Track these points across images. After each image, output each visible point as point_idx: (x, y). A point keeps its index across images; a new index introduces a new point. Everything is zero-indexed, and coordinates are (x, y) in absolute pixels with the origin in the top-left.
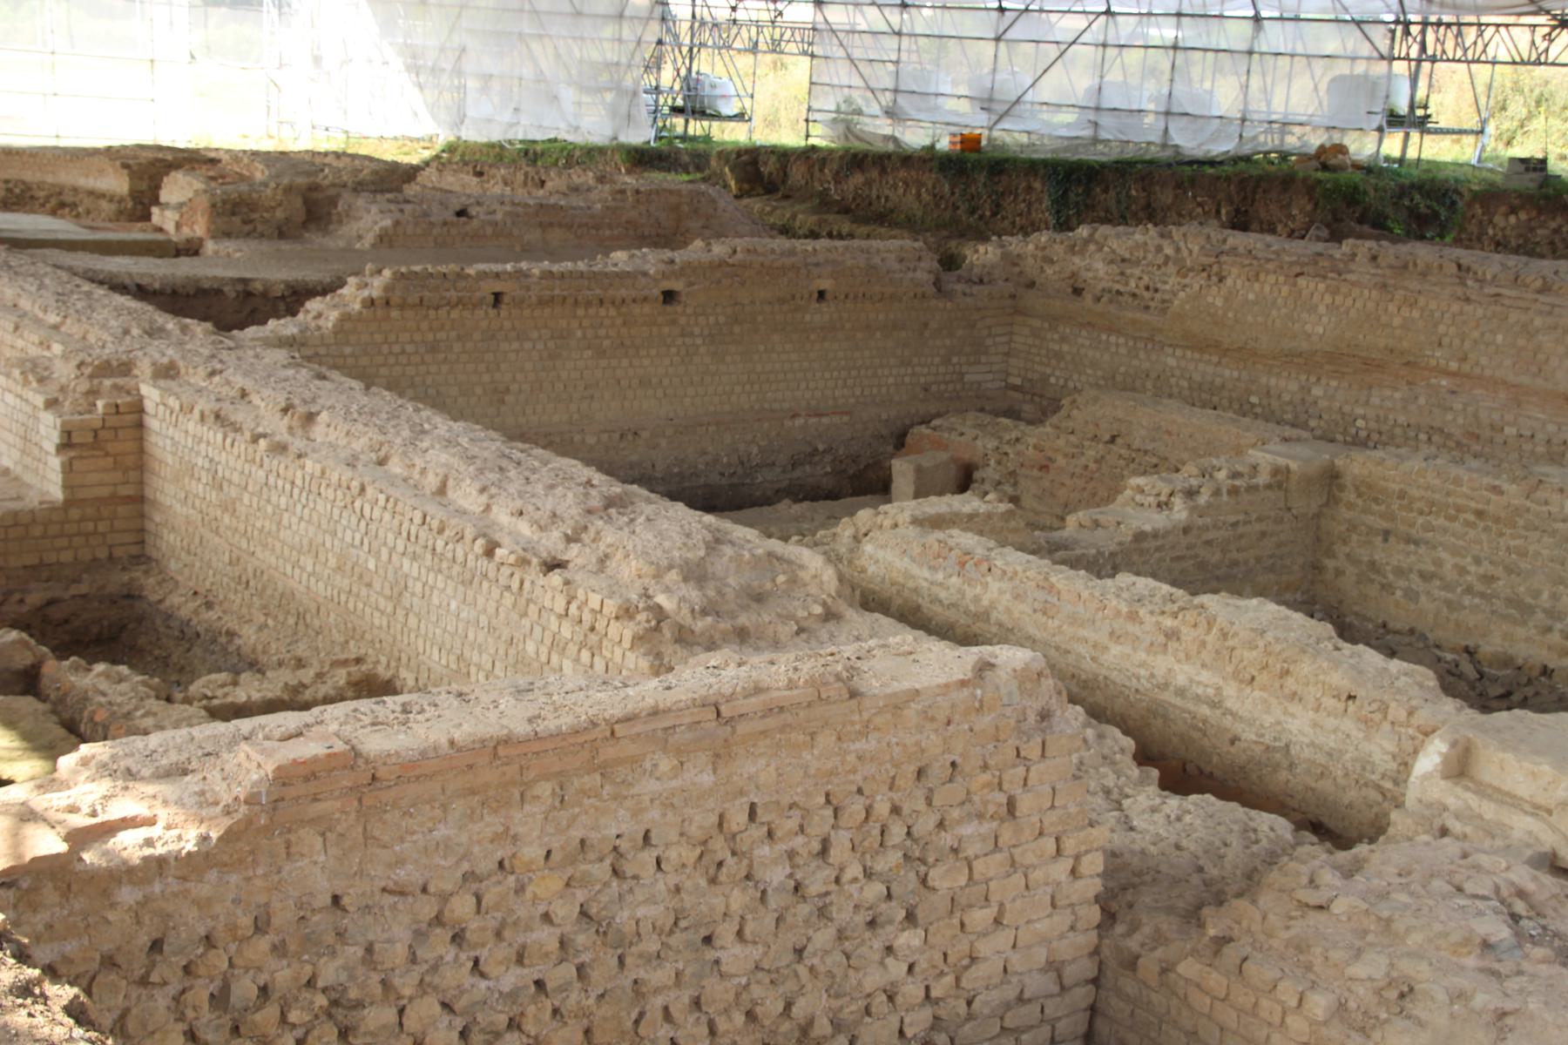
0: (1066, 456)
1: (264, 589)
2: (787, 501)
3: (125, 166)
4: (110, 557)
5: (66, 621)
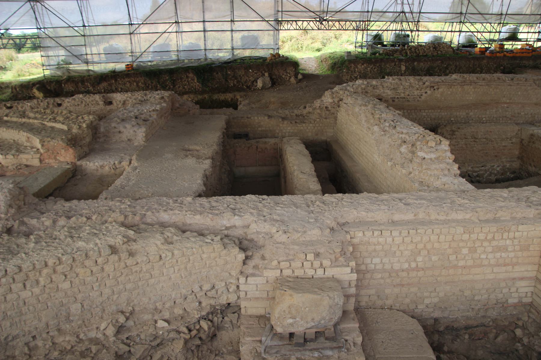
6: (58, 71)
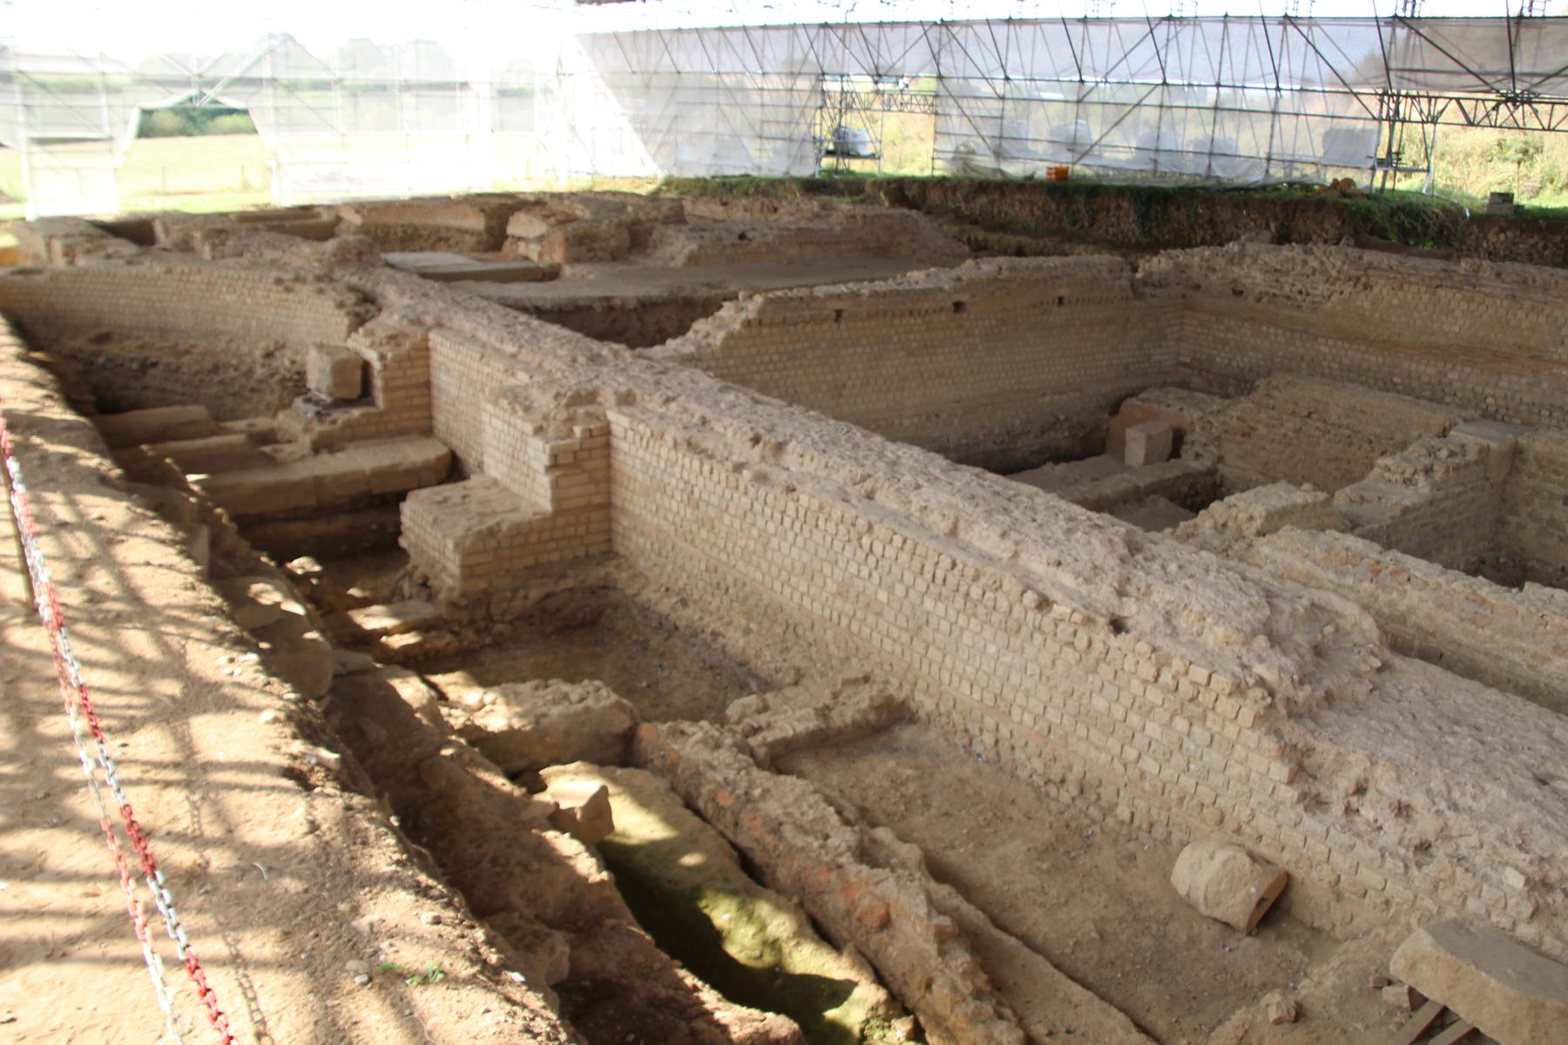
0: (1267, 426)
1: (746, 598)
2: (1050, 465)
3: (482, 210)
4: (588, 556)
5: (558, 610)
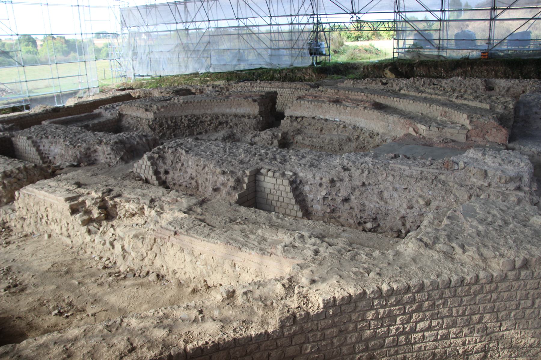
3: (255, 101)
6: (408, 55)
